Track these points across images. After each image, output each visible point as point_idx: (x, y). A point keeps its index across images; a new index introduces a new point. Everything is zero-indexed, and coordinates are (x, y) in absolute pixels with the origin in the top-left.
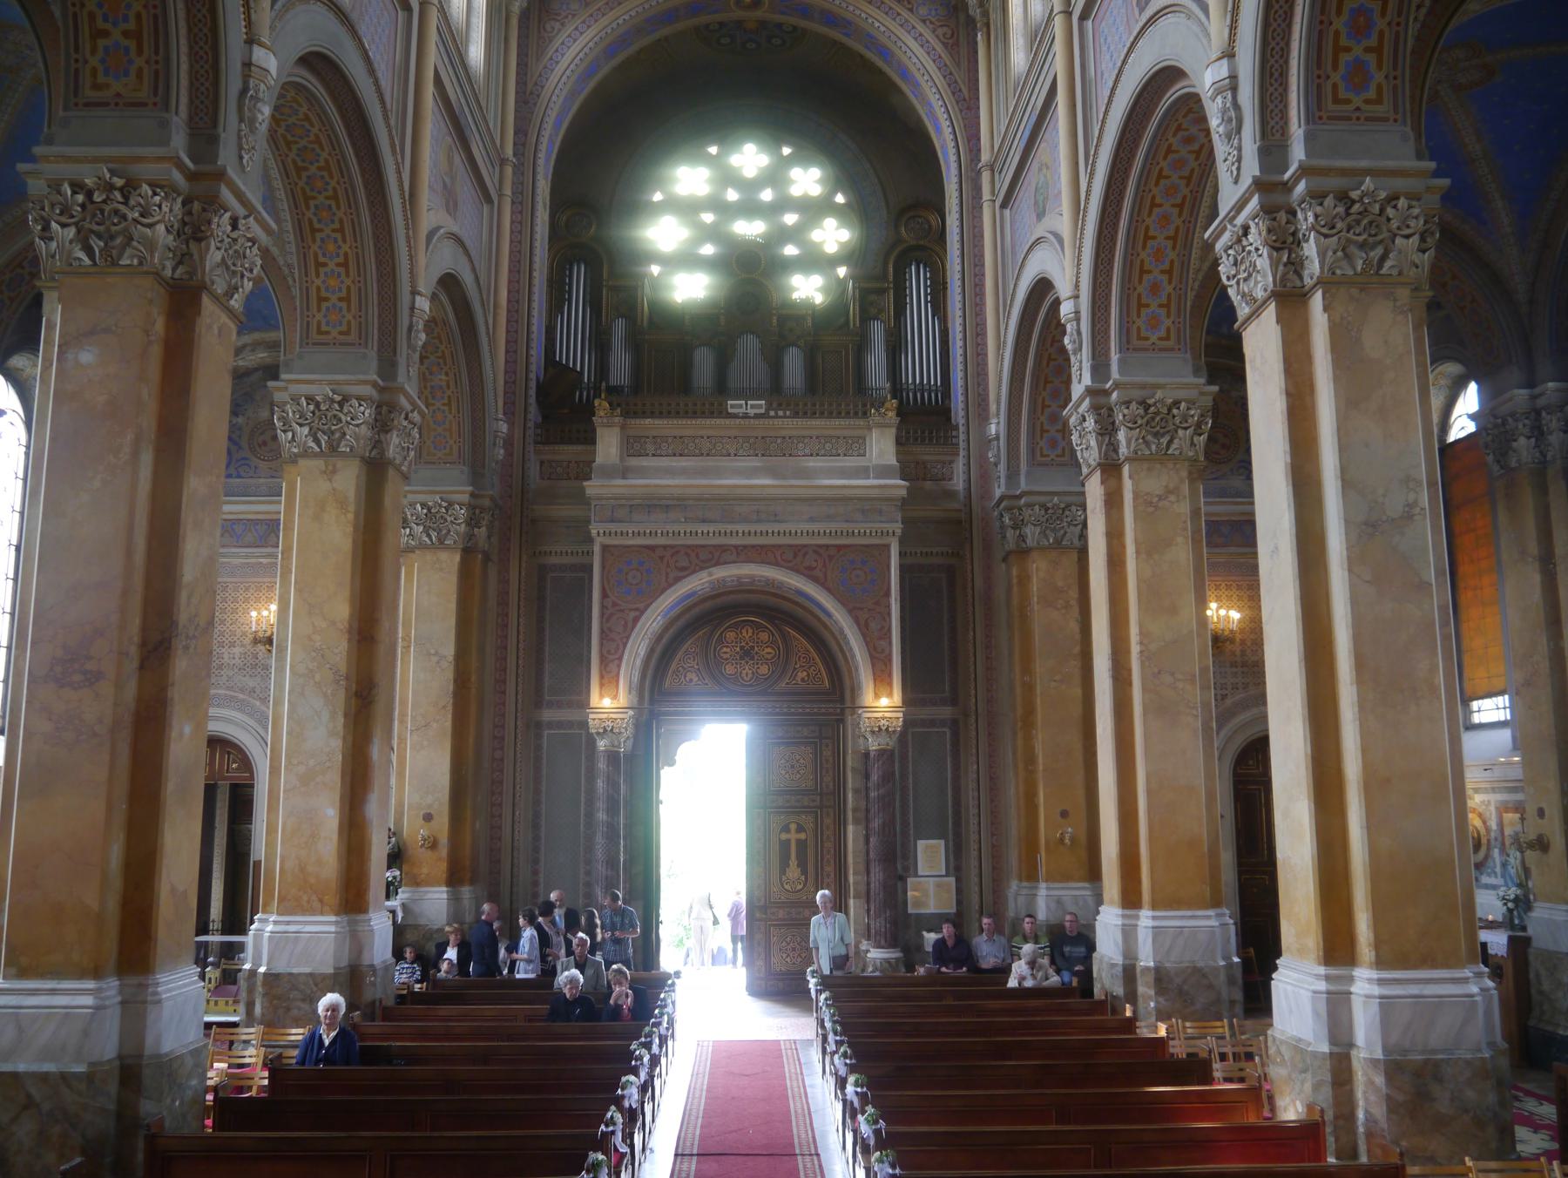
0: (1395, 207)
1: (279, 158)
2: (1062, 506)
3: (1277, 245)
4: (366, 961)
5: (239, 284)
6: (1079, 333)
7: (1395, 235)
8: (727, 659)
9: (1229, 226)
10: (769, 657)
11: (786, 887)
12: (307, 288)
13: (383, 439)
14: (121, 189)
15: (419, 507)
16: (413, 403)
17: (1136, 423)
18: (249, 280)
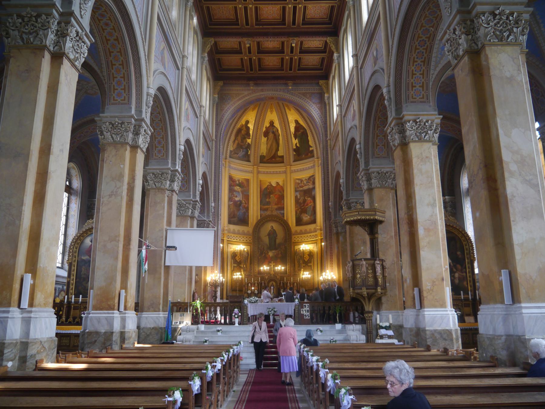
0: (513, 16)
1: (100, 35)
2: (385, 172)
3: (468, 33)
4: (126, 330)
5: (79, 57)
6: (390, 98)
7: (513, 27)
9: (448, 31)
12: (109, 74)
13: (136, 138)
14: (35, 17)
15: (151, 174)
16: (147, 126)
17: (412, 128)
18: (83, 57)
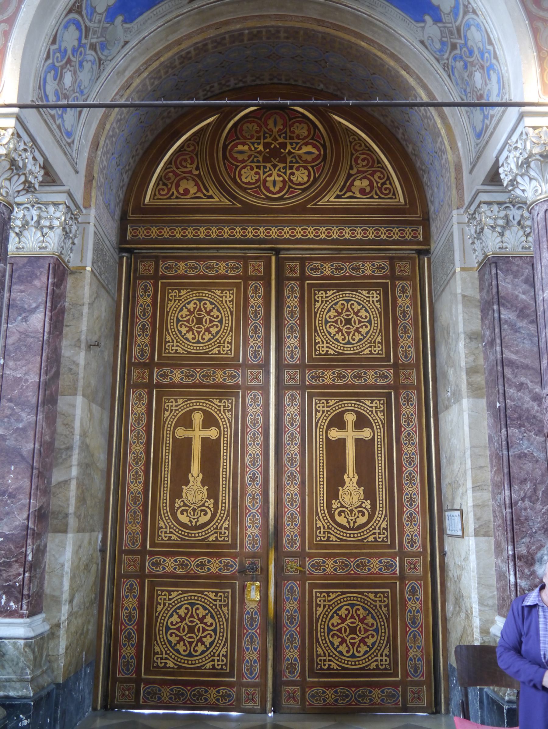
8: (243, 161)
10: (309, 158)
11: (339, 519)
